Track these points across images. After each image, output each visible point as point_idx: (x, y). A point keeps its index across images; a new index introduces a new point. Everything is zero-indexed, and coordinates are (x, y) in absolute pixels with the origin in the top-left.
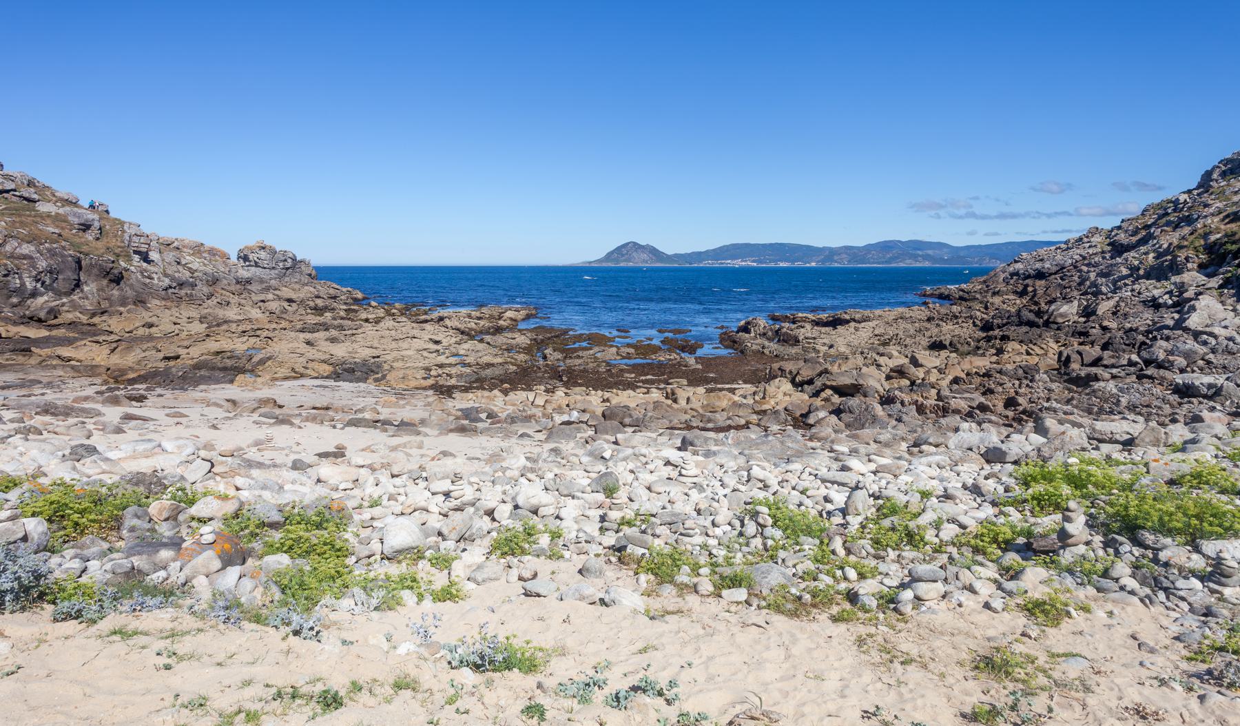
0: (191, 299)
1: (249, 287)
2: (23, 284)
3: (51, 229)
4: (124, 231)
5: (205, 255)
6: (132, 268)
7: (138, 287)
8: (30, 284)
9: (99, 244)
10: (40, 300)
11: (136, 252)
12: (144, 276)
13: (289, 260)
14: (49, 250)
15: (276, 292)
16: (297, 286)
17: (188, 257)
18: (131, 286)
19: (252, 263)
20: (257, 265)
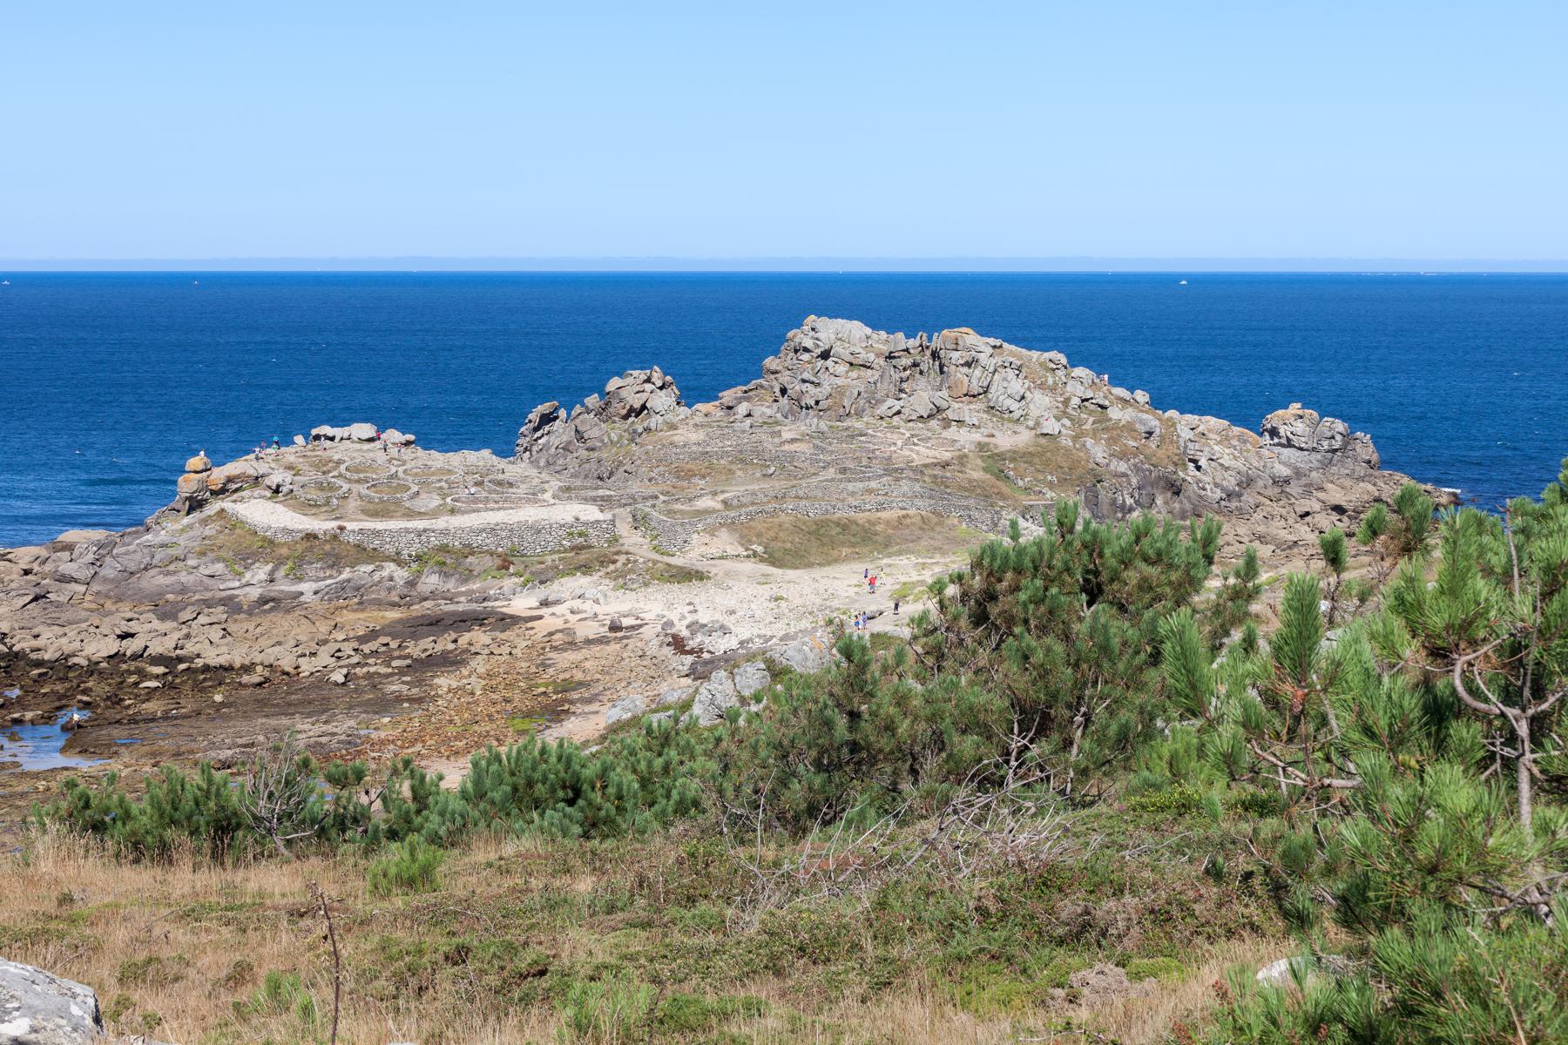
0: (1241, 513)
1: (1288, 490)
2: (1124, 501)
3: (1132, 443)
4: (1178, 436)
5: (1234, 442)
6: (1189, 479)
7: (1195, 499)
8: (1129, 501)
9: (1161, 453)
10: (1135, 514)
11: (1190, 460)
12: (1200, 488)
13: (1339, 437)
14: (1135, 465)
15: (1321, 495)
16: (1348, 483)
17: (1216, 448)
18: (1188, 498)
19: (1284, 441)
20: (1289, 444)
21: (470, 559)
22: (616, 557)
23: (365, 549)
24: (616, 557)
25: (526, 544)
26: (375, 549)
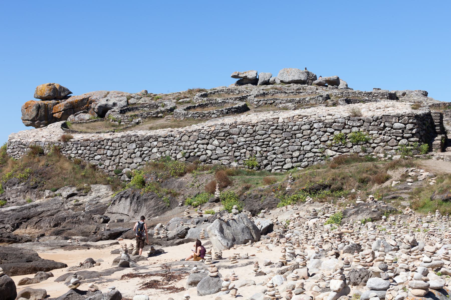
21: (188, 178)
22: (390, 173)
23: (83, 167)
24: (390, 173)
25: (271, 156)
26: (94, 167)
